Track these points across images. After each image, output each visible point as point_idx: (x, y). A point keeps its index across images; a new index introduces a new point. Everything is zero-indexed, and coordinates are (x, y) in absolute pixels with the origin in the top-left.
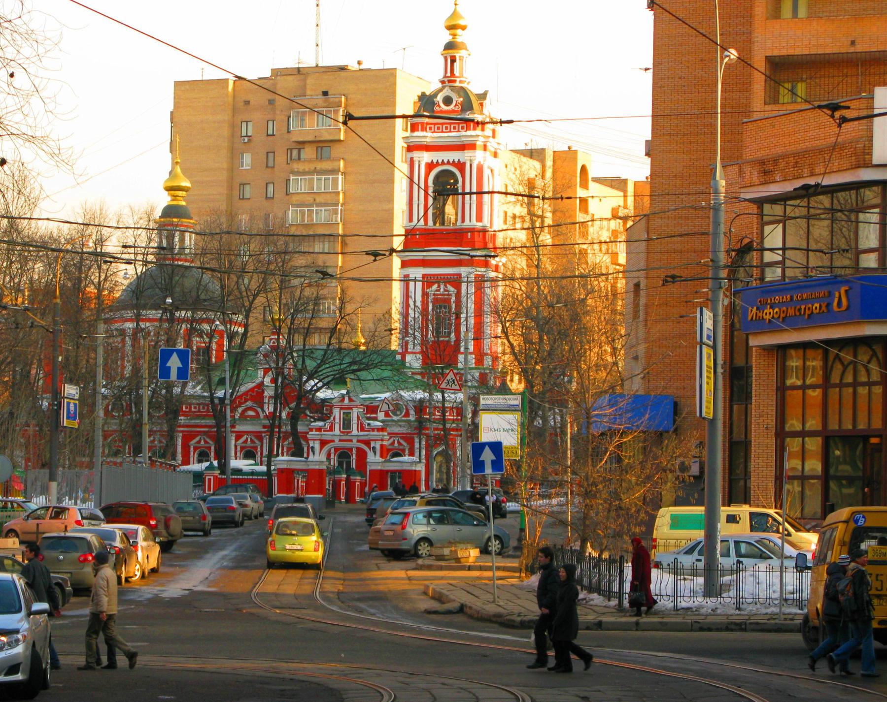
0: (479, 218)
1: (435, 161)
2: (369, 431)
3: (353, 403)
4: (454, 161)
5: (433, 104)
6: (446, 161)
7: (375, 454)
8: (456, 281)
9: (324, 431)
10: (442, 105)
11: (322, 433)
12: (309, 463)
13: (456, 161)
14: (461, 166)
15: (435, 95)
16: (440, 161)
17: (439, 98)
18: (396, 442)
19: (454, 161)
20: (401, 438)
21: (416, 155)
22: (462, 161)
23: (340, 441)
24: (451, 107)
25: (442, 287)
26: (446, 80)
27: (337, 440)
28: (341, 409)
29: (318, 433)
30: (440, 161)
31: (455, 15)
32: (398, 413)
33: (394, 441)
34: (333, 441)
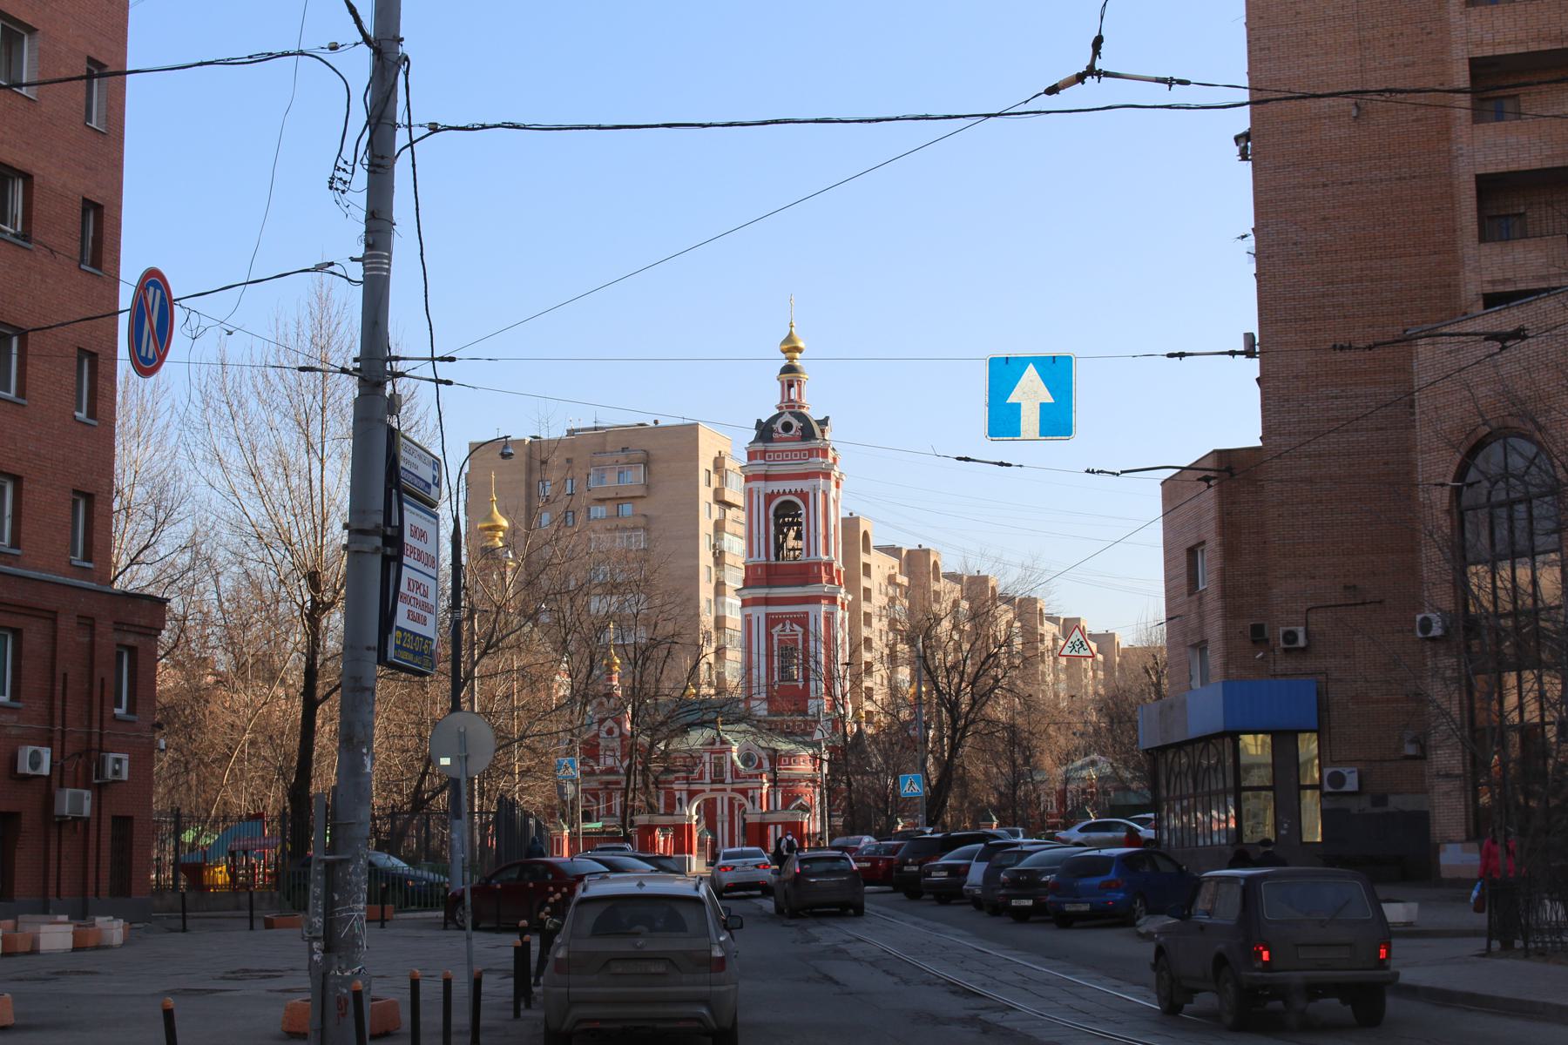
0: (827, 553)
1: (776, 491)
3: (725, 746)
5: (772, 431)
6: (787, 491)
8: (803, 621)
10: (780, 430)
13: (799, 490)
14: (803, 496)
15: (774, 419)
16: (781, 491)
17: (778, 426)
21: (755, 485)
23: (712, 790)
24: (792, 432)
25: (788, 626)
26: (783, 405)
28: (712, 753)
30: (781, 491)
31: (790, 338)
32: (750, 763)
34: (704, 791)
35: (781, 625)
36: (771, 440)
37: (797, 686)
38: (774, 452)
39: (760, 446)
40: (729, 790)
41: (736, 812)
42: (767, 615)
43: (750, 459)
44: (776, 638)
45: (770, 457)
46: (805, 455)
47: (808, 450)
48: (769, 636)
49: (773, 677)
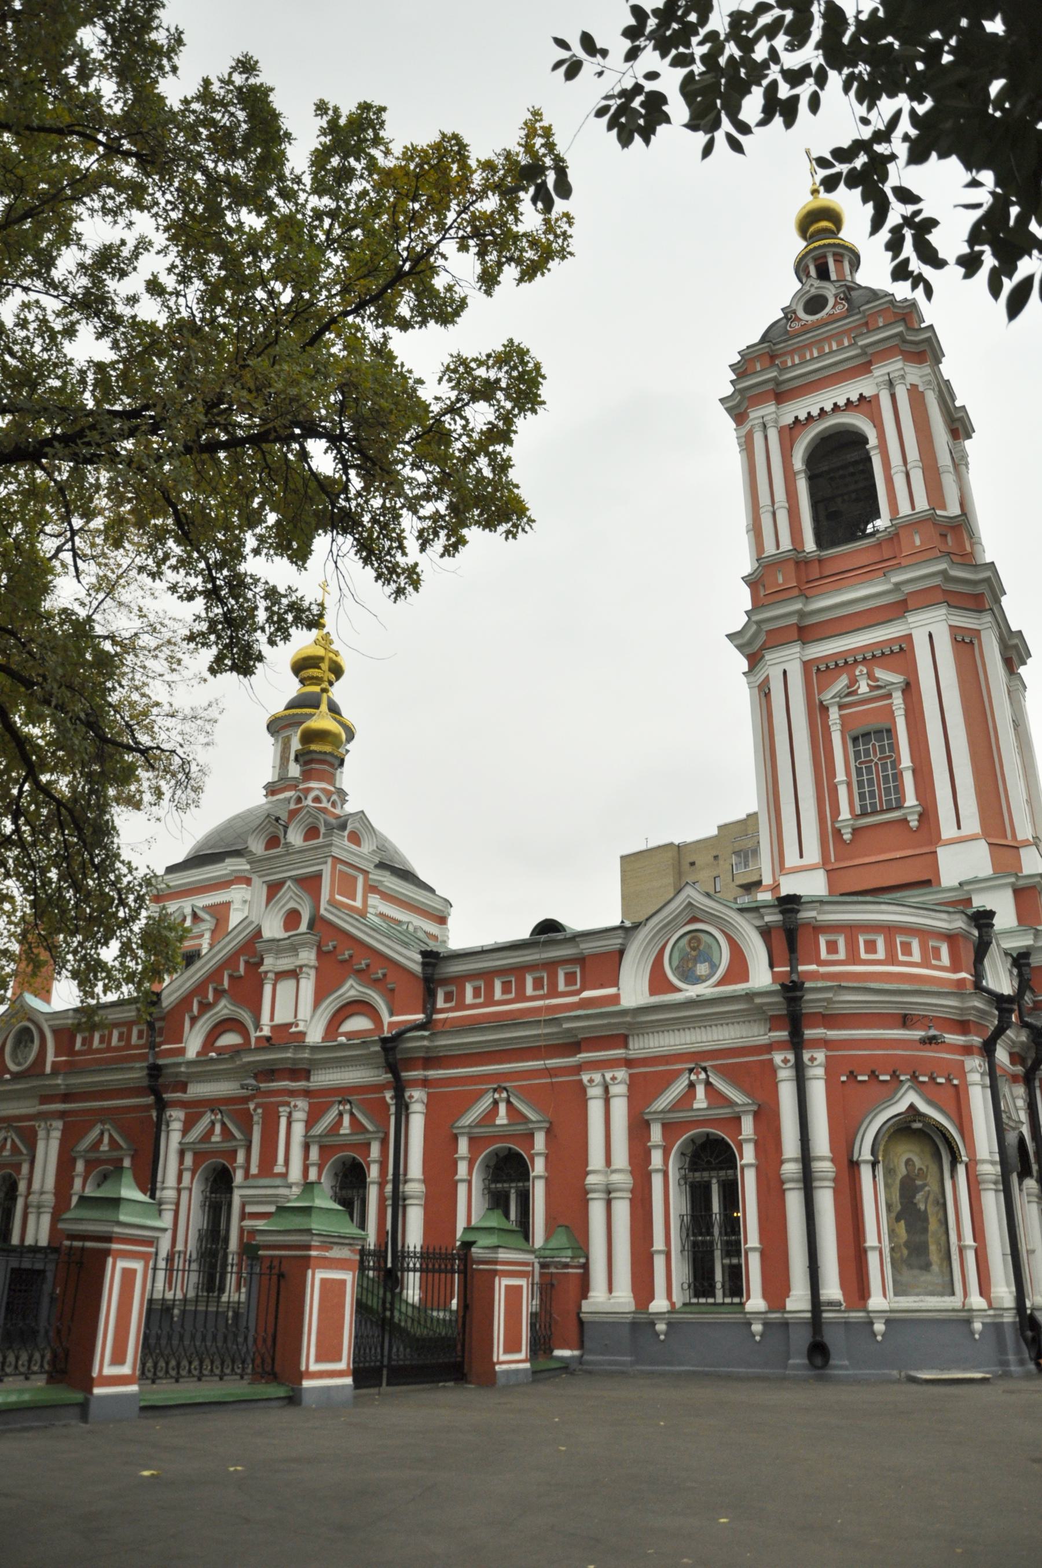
1: (802, 417)
4: (849, 402)
6: (828, 407)
10: (801, 314)
13: (854, 398)
14: (866, 404)
16: (815, 412)
18: (700, 1091)
19: (849, 402)
20: (720, 1070)
22: (866, 394)
24: (828, 309)
30: (815, 412)
32: (702, 969)
33: (692, 1085)
35: (843, 681)
37: (905, 821)
41: (657, 1158)
42: (806, 665)
44: (834, 714)
48: (817, 711)
49: (836, 811)
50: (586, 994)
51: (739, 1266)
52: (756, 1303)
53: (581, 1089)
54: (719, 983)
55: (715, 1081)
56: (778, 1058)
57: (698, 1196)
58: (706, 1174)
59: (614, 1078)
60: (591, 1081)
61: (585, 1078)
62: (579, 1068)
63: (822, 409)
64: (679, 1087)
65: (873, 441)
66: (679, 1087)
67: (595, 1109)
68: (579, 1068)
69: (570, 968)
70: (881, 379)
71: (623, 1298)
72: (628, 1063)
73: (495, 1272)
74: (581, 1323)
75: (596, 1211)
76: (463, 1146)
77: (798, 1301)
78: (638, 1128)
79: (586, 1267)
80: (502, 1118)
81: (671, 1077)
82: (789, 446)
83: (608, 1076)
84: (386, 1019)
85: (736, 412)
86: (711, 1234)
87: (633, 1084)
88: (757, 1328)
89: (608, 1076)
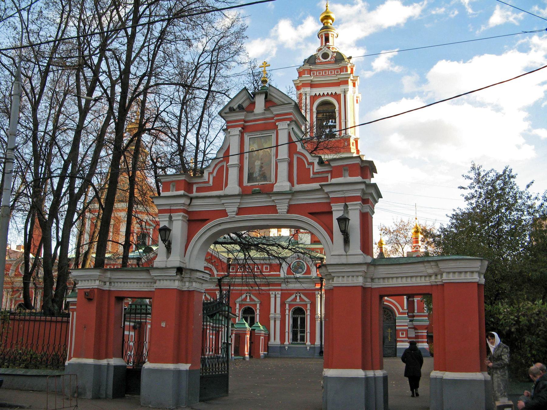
1: (318, 94)
2: (326, 179)
3: (276, 111)
6: (326, 94)
7: (347, 241)
9: (199, 190)
10: (321, 58)
11: (195, 194)
12: (153, 273)
13: (334, 93)
14: (337, 96)
16: (321, 94)
18: (298, 298)
22: (338, 93)
27: (232, 209)
29: (181, 192)
30: (321, 94)
32: (300, 270)
33: (296, 296)
36: (315, 63)
38: (317, 71)
39: (307, 67)
40: (282, 208)
41: (287, 311)
43: (300, 76)
45: (314, 74)
46: (337, 72)
47: (340, 69)
50: (272, 273)
51: (304, 336)
52: (308, 343)
53: (269, 296)
54: (304, 274)
55: (302, 296)
56: (317, 292)
57: (295, 320)
58: (297, 316)
59: (278, 293)
60: (272, 293)
61: (271, 292)
62: (270, 290)
63: (324, 93)
64: (293, 297)
65: (337, 109)
66: (293, 297)
67: (272, 300)
68: (270, 290)
69: (266, 266)
70: (342, 90)
71: (278, 341)
72: (282, 290)
73: (260, 336)
74: (268, 347)
75: (272, 322)
76: (238, 306)
77: (318, 342)
78: (283, 305)
79: (269, 334)
80: (248, 300)
81: (291, 294)
82: (312, 103)
83: (277, 293)
84: (215, 273)
85: (297, 85)
86: (298, 328)
87: (282, 294)
88: (308, 348)
89: (277, 293)
